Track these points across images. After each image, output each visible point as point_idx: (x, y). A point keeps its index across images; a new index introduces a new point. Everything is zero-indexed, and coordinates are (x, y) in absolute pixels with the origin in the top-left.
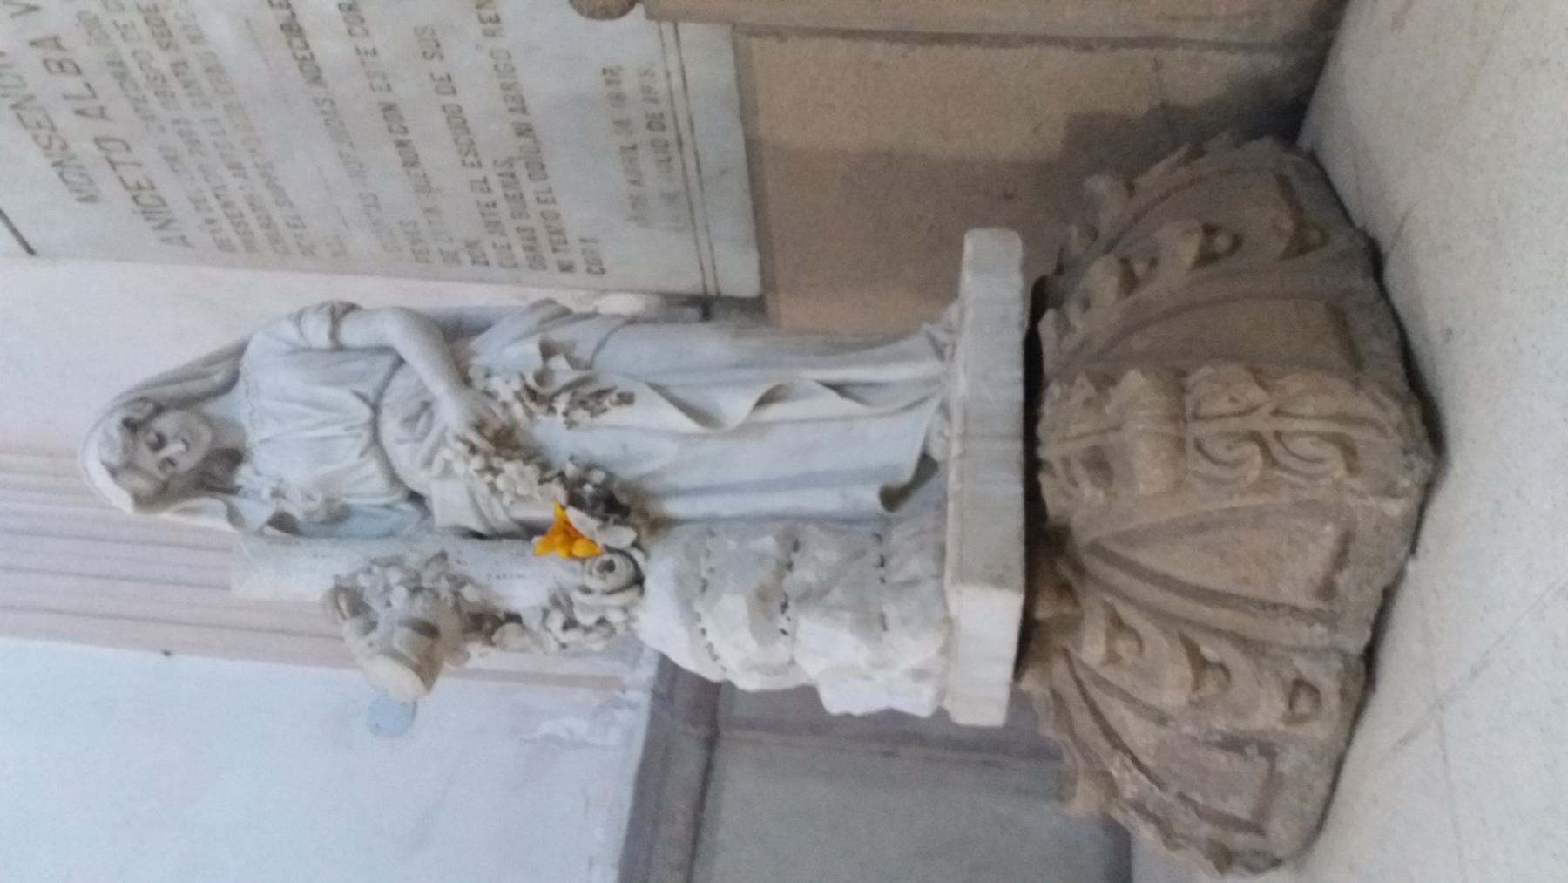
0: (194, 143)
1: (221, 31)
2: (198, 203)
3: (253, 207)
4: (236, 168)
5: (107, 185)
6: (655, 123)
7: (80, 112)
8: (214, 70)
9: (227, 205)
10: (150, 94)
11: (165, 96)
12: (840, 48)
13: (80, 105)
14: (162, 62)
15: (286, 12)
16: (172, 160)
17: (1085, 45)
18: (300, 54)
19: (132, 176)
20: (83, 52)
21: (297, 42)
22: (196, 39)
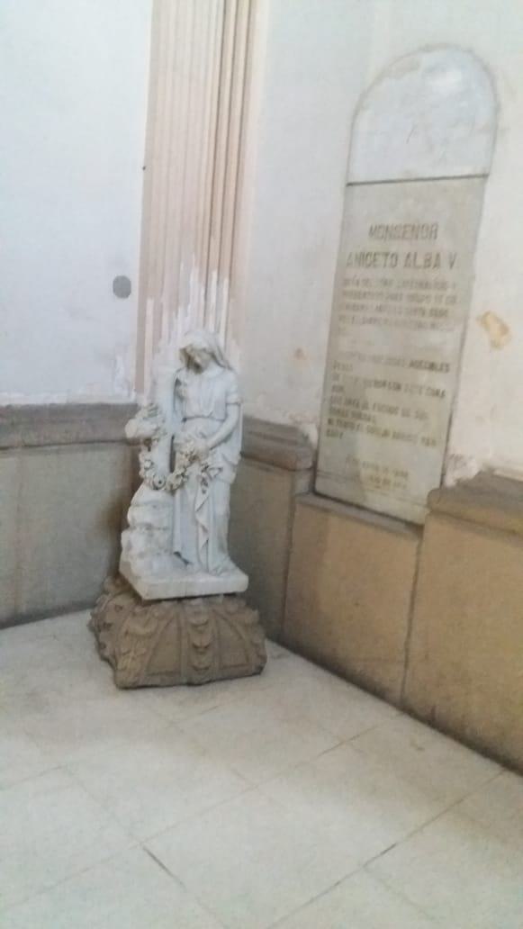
0: (394, 297)
1: (434, 337)
2: (366, 282)
3: (363, 307)
4: (380, 309)
5: (374, 246)
6: (386, 482)
7: (408, 256)
8: (420, 326)
9: (365, 294)
10: (413, 292)
11: (412, 298)
12: (412, 571)
13: (412, 258)
14: (424, 305)
15: (439, 367)
16: (386, 283)
17: (407, 643)
18: (423, 364)
19: (381, 259)
20: (432, 275)
21: (428, 366)
22: (433, 326)
